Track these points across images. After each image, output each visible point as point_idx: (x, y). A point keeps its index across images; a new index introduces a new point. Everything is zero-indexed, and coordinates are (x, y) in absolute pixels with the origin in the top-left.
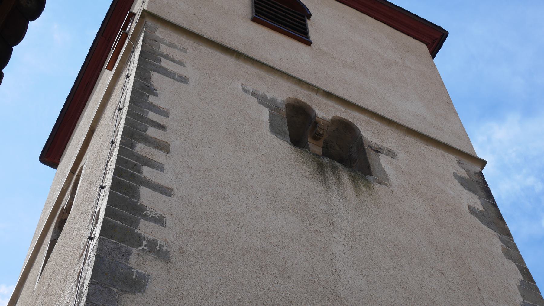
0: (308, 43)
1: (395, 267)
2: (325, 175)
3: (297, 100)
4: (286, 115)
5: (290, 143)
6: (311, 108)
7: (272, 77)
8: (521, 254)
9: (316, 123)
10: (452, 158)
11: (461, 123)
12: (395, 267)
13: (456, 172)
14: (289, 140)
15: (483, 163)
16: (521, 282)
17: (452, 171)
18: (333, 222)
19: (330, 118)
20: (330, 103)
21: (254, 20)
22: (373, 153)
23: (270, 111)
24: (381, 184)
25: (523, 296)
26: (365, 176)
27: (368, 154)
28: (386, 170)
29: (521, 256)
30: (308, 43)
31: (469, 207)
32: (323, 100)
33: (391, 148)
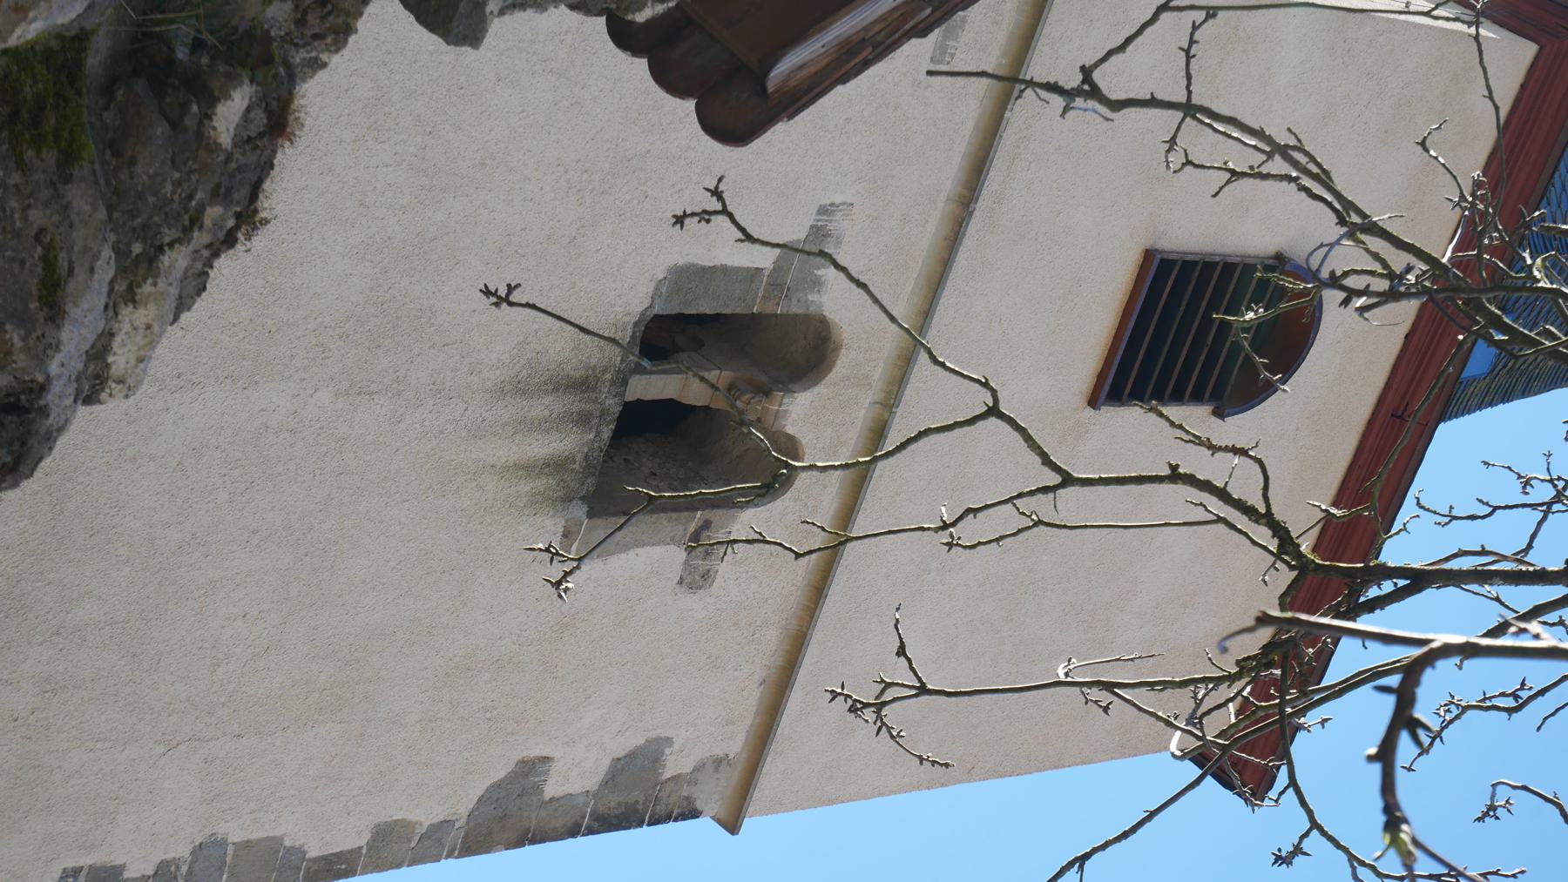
0: (1093, 402)
1: (255, 532)
2: (547, 392)
3: (838, 347)
4: (760, 314)
5: (651, 314)
6: (816, 383)
7: (909, 287)
8: (404, 870)
9: (767, 393)
10: (735, 744)
11: (894, 793)
12: (255, 532)
13: (676, 746)
14: (656, 310)
15: (732, 825)
16: (300, 852)
17: (680, 736)
18: (371, 394)
19: (790, 430)
20: (1524, 589)
21: (1149, 254)
22: (692, 528)
23: (766, 273)
24: (565, 536)
25: (247, 844)
26: (583, 499)
27: (674, 515)
28: (623, 556)
29: (399, 866)
30: (1093, 402)
31: (546, 760)
32: (860, 416)
33: (718, 581)
